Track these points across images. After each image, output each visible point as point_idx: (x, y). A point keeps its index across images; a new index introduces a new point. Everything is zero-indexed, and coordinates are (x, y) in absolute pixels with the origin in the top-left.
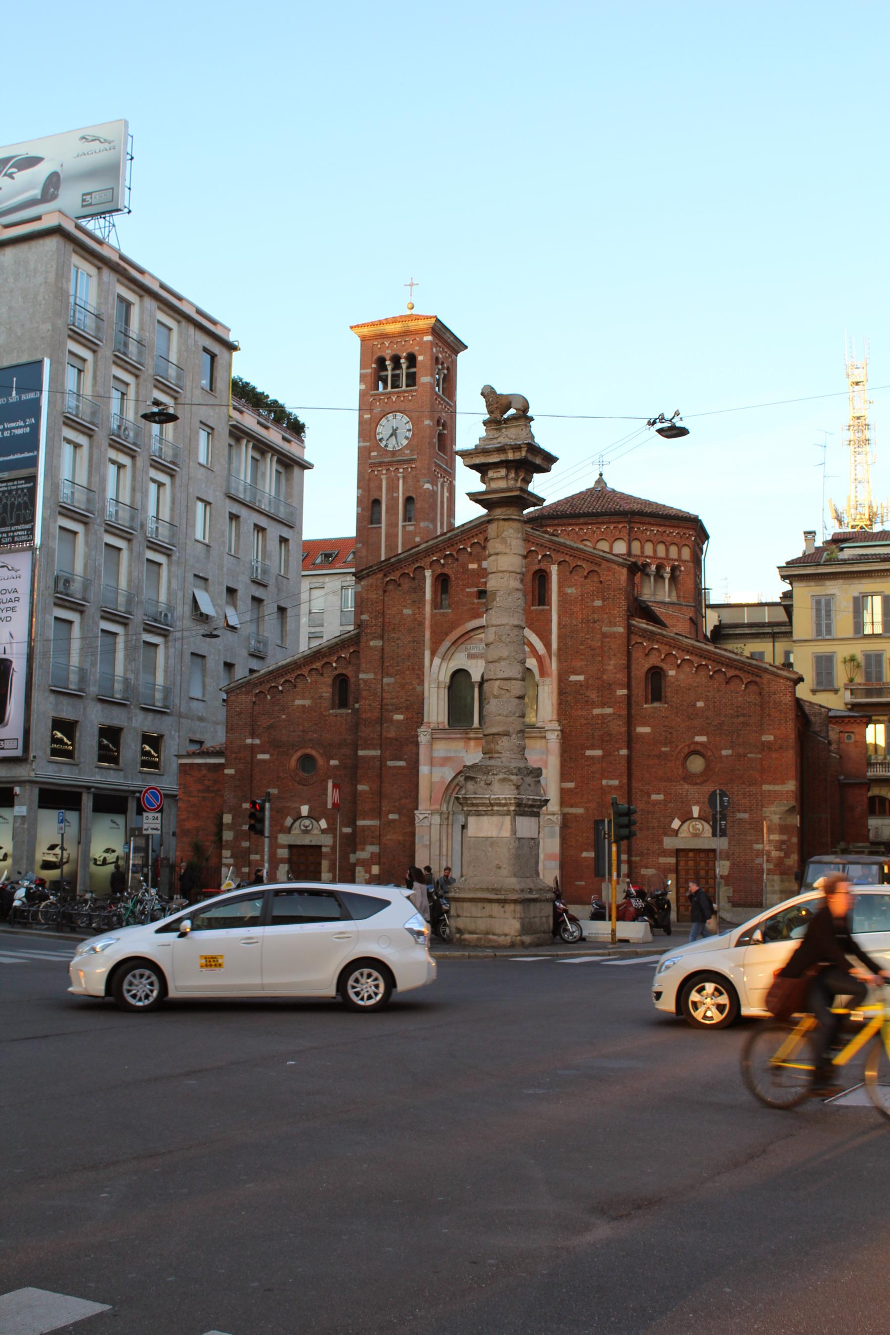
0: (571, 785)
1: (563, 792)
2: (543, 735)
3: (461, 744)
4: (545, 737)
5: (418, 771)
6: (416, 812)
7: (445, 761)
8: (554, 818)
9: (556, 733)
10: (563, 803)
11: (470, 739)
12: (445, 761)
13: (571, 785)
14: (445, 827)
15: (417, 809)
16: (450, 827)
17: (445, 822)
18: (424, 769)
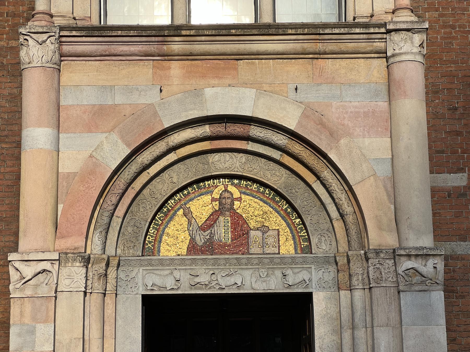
0: (458, 180)
1: (439, 197)
2: (379, 45)
3: (144, 72)
4: (382, 54)
5: (19, 145)
6: (12, 257)
7: (99, 117)
8: (427, 267)
9: (418, 38)
10: (441, 231)
11: (168, 56)
12: (99, 117)
13: (458, 180)
14: (94, 299)
15: (15, 249)
16: (109, 300)
17: (98, 286)
18: (36, 137)
